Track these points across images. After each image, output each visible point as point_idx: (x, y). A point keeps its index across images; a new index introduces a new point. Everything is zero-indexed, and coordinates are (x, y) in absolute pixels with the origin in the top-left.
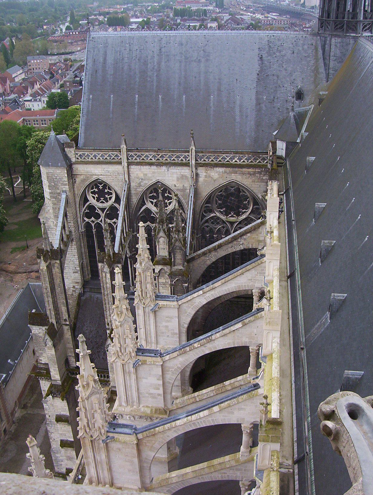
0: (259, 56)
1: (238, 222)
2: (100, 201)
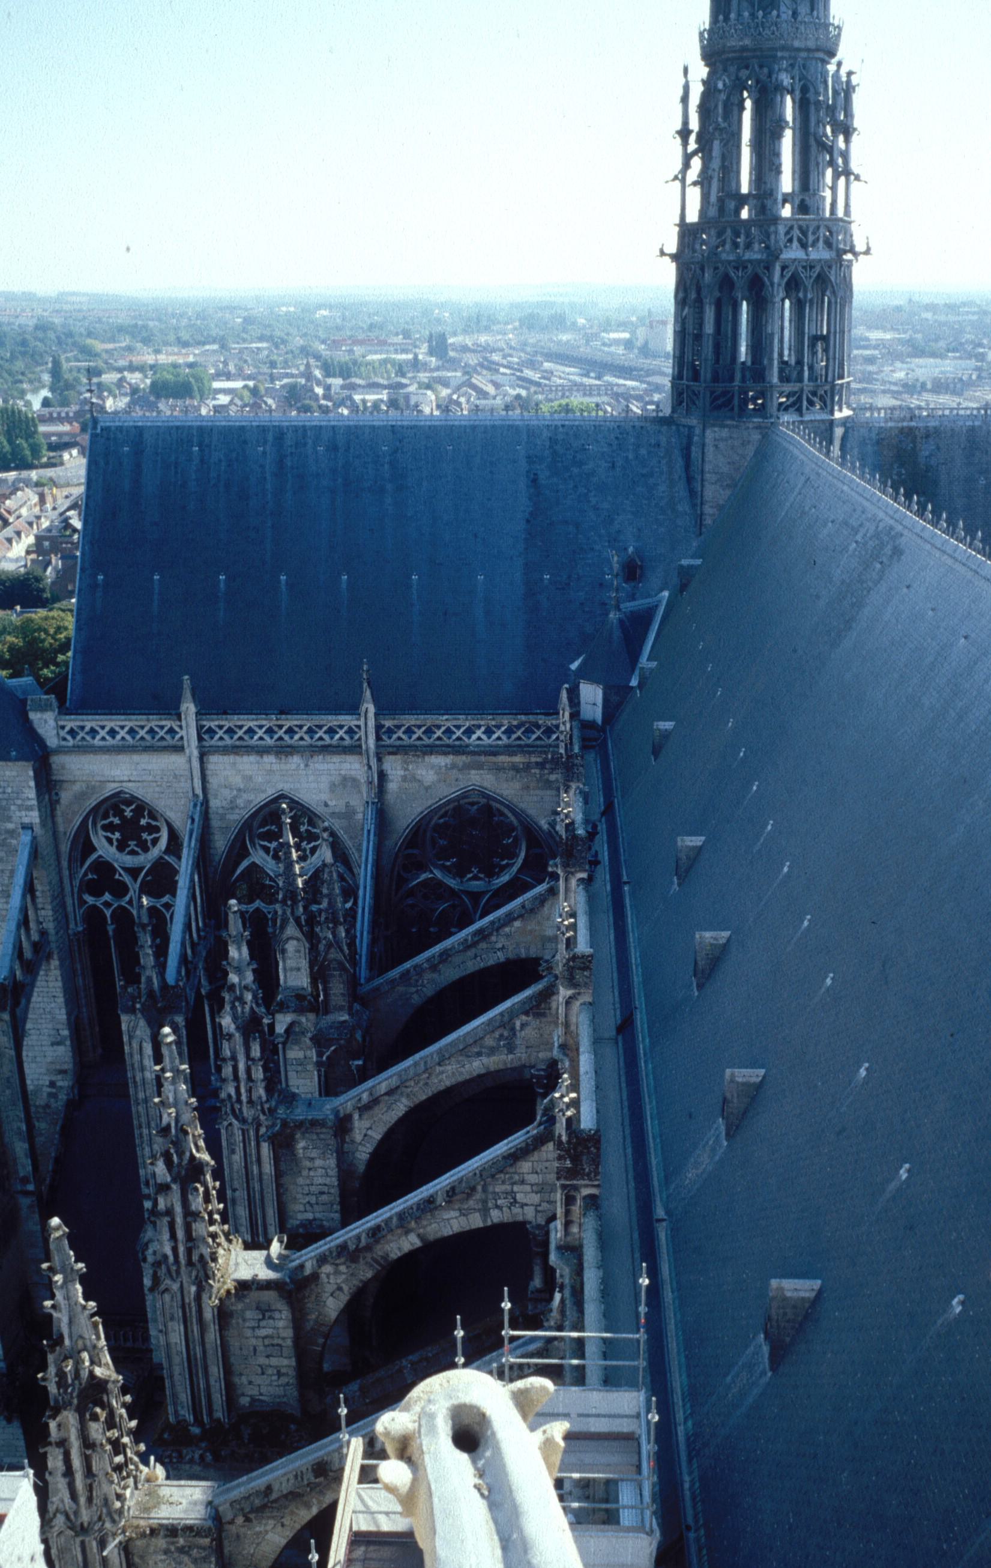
0: (527, 476)
1: (488, 891)
2: (128, 849)
